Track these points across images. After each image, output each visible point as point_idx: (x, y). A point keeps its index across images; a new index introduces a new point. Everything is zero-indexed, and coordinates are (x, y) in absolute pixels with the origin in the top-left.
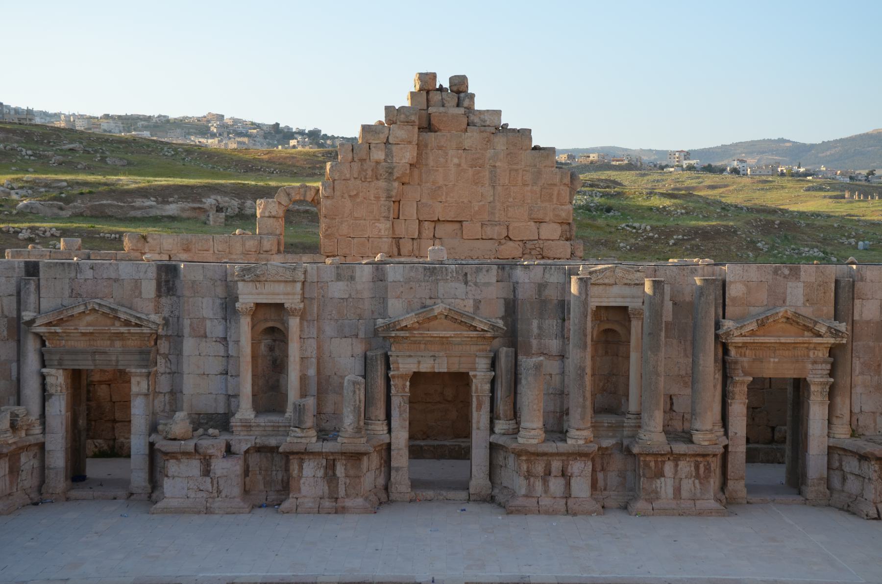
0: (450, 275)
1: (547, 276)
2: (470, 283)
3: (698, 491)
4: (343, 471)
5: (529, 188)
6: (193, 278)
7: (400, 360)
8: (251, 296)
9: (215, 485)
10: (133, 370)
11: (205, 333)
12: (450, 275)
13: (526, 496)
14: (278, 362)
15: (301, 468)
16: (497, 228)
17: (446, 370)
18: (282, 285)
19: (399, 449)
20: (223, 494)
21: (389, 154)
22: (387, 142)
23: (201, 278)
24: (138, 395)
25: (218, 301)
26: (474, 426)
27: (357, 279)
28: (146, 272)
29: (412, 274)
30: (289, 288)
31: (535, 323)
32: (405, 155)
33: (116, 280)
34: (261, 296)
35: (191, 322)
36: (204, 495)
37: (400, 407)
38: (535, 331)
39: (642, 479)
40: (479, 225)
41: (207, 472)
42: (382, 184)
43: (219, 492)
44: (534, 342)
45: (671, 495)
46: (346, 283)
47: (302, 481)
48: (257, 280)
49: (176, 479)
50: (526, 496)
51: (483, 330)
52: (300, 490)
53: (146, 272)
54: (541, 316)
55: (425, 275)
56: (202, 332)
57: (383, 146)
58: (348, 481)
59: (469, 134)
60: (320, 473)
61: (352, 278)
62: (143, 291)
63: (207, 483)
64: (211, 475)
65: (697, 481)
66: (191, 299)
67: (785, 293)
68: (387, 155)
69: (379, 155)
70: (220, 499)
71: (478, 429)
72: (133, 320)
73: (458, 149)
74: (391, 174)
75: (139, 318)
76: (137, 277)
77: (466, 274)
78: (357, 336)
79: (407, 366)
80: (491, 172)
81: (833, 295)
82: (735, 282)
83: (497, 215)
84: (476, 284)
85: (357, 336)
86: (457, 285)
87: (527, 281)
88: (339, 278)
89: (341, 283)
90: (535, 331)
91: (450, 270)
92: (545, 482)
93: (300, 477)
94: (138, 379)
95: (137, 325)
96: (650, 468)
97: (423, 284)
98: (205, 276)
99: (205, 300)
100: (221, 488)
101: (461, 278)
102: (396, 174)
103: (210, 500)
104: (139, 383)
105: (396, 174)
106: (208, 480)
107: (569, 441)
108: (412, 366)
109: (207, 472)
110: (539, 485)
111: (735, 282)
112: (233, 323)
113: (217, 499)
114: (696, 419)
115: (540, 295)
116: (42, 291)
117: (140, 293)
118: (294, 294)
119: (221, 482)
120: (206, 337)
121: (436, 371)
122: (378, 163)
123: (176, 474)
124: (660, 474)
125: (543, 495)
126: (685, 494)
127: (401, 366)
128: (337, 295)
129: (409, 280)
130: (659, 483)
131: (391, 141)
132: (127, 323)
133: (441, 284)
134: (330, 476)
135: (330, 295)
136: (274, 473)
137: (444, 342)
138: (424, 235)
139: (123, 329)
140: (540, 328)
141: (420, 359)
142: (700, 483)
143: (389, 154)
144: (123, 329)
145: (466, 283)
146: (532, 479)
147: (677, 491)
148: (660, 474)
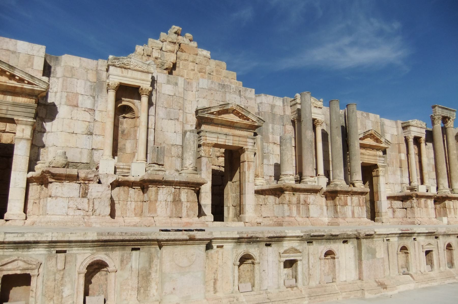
0: (232, 90)
1: (275, 101)
2: (242, 97)
3: (361, 213)
4: (185, 197)
6: (72, 65)
7: (207, 134)
8: (118, 78)
9: (91, 205)
10: (20, 119)
11: (77, 104)
12: (232, 90)
13: (289, 216)
14: (126, 132)
15: (157, 193)
17: (231, 144)
18: (140, 73)
19: (206, 192)
20: (98, 212)
22: (161, 49)
23: (78, 66)
24: (22, 139)
25: (89, 83)
26: (247, 179)
27: (179, 85)
28: (38, 51)
29: (213, 86)
30: (144, 76)
31: (270, 126)
33: (14, 52)
34: (125, 79)
35: (67, 95)
36: (81, 213)
37: (206, 164)
38: (271, 130)
39: (339, 207)
41: (85, 195)
43: (94, 211)
44: (271, 136)
45: (351, 216)
46: (173, 86)
47: (157, 204)
48: (124, 67)
49: (59, 199)
50: (289, 216)
51: (253, 121)
52: (156, 211)
53: (38, 51)
54: (273, 123)
55: (219, 88)
56: (75, 103)
58: (189, 204)
60: (170, 198)
61: (176, 84)
62: (35, 64)
63: (84, 203)
64: (88, 196)
65: (360, 208)
66: (69, 79)
68: (161, 56)
70: (94, 217)
71: (249, 182)
72: (27, 78)
73: (193, 62)
75: (32, 77)
76: (31, 54)
77: (240, 91)
78: (178, 119)
79: (211, 139)
84: (245, 97)
85: (178, 119)
86: (235, 96)
87: (266, 102)
88: (168, 82)
89: (169, 86)
90: (271, 130)
91: (232, 87)
93: (156, 201)
94: (23, 127)
95: (29, 83)
96: (342, 200)
97: (218, 92)
98: (81, 66)
99: (79, 81)
100: (96, 207)
101: (237, 92)
103: (86, 217)
104: (23, 130)
106: (86, 200)
107: (309, 183)
108: (214, 139)
109: (85, 195)
110: (294, 209)
112: (100, 98)
113: (92, 217)
114: (356, 175)
117: (32, 65)
118: (147, 81)
119: (96, 203)
120: (77, 106)
121: (227, 144)
123: (58, 195)
124: (346, 204)
125: (297, 216)
126: (356, 215)
127: (208, 138)
128: (167, 93)
129: (210, 89)
131: (164, 49)
132: (21, 80)
133: (228, 94)
134: (177, 201)
135: (163, 92)
136: (129, 203)
137: (231, 125)
139: (19, 85)
140: (273, 129)
141: (219, 135)
142: (361, 209)
144: (19, 85)
146: (291, 205)
147: (353, 213)
148: (346, 204)
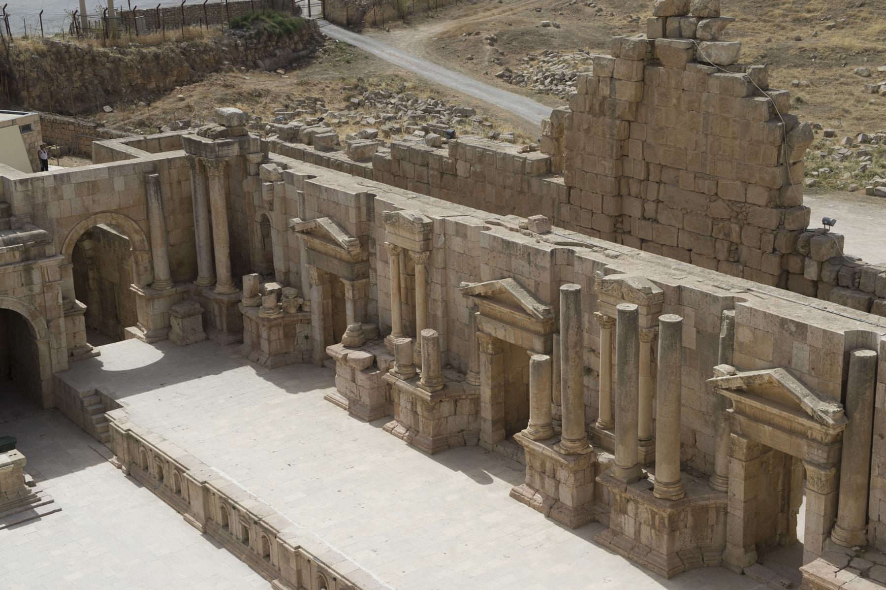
5: (738, 142)
16: (707, 183)
21: (613, 90)
32: (627, 92)
40: (692, 176)
42: (608, 120)
57: (608, 80)
59: (687, 73)
65: (653, 531)
67: (790, 352)
68: (611, 91)
69: (605, 90)
74: (614, 111)
80: (704, 119)
81: (840, 370)
82: (743, 325)
83: (708, 168)
87: (580, 272)
92: (542, 479)
102: (618, 113)
105: (618, 113)
111: (743, 325)
115: (590, 289)
116: (306, 203)
122: (604, 98)
130: (623, 519)
138: (651, 178)
143: (613, 90)
145: (529, 263)
